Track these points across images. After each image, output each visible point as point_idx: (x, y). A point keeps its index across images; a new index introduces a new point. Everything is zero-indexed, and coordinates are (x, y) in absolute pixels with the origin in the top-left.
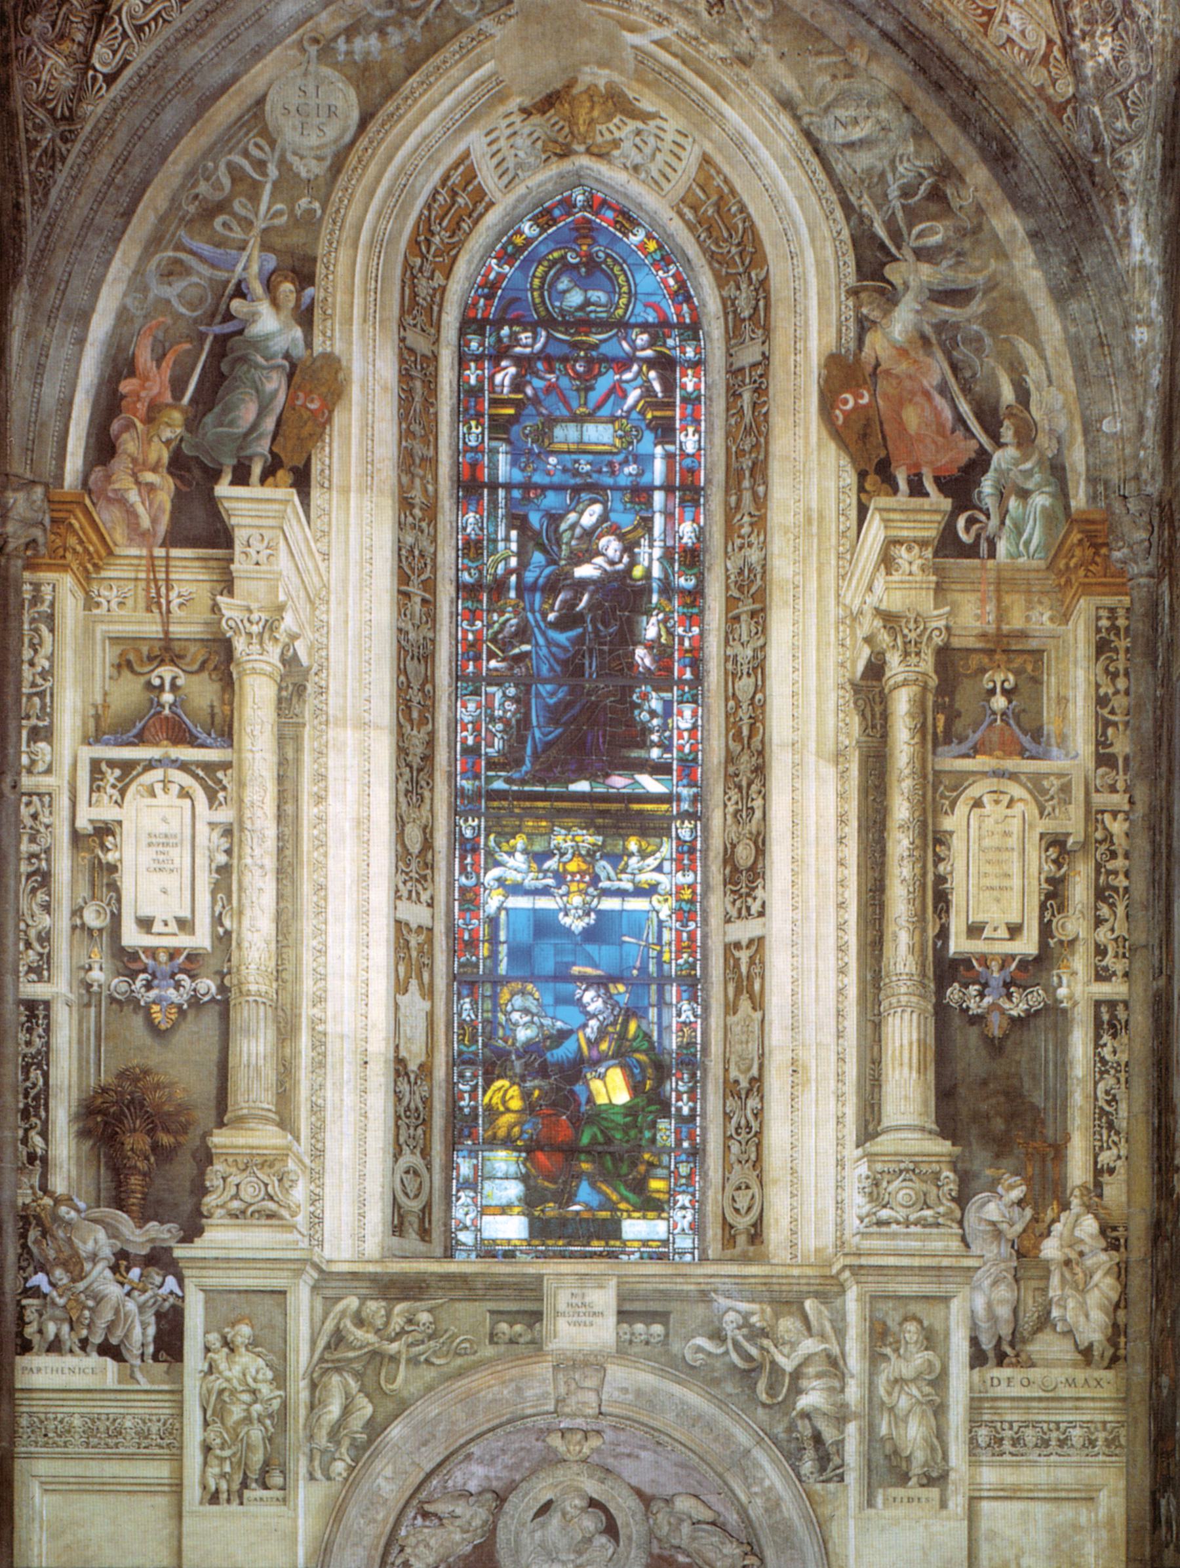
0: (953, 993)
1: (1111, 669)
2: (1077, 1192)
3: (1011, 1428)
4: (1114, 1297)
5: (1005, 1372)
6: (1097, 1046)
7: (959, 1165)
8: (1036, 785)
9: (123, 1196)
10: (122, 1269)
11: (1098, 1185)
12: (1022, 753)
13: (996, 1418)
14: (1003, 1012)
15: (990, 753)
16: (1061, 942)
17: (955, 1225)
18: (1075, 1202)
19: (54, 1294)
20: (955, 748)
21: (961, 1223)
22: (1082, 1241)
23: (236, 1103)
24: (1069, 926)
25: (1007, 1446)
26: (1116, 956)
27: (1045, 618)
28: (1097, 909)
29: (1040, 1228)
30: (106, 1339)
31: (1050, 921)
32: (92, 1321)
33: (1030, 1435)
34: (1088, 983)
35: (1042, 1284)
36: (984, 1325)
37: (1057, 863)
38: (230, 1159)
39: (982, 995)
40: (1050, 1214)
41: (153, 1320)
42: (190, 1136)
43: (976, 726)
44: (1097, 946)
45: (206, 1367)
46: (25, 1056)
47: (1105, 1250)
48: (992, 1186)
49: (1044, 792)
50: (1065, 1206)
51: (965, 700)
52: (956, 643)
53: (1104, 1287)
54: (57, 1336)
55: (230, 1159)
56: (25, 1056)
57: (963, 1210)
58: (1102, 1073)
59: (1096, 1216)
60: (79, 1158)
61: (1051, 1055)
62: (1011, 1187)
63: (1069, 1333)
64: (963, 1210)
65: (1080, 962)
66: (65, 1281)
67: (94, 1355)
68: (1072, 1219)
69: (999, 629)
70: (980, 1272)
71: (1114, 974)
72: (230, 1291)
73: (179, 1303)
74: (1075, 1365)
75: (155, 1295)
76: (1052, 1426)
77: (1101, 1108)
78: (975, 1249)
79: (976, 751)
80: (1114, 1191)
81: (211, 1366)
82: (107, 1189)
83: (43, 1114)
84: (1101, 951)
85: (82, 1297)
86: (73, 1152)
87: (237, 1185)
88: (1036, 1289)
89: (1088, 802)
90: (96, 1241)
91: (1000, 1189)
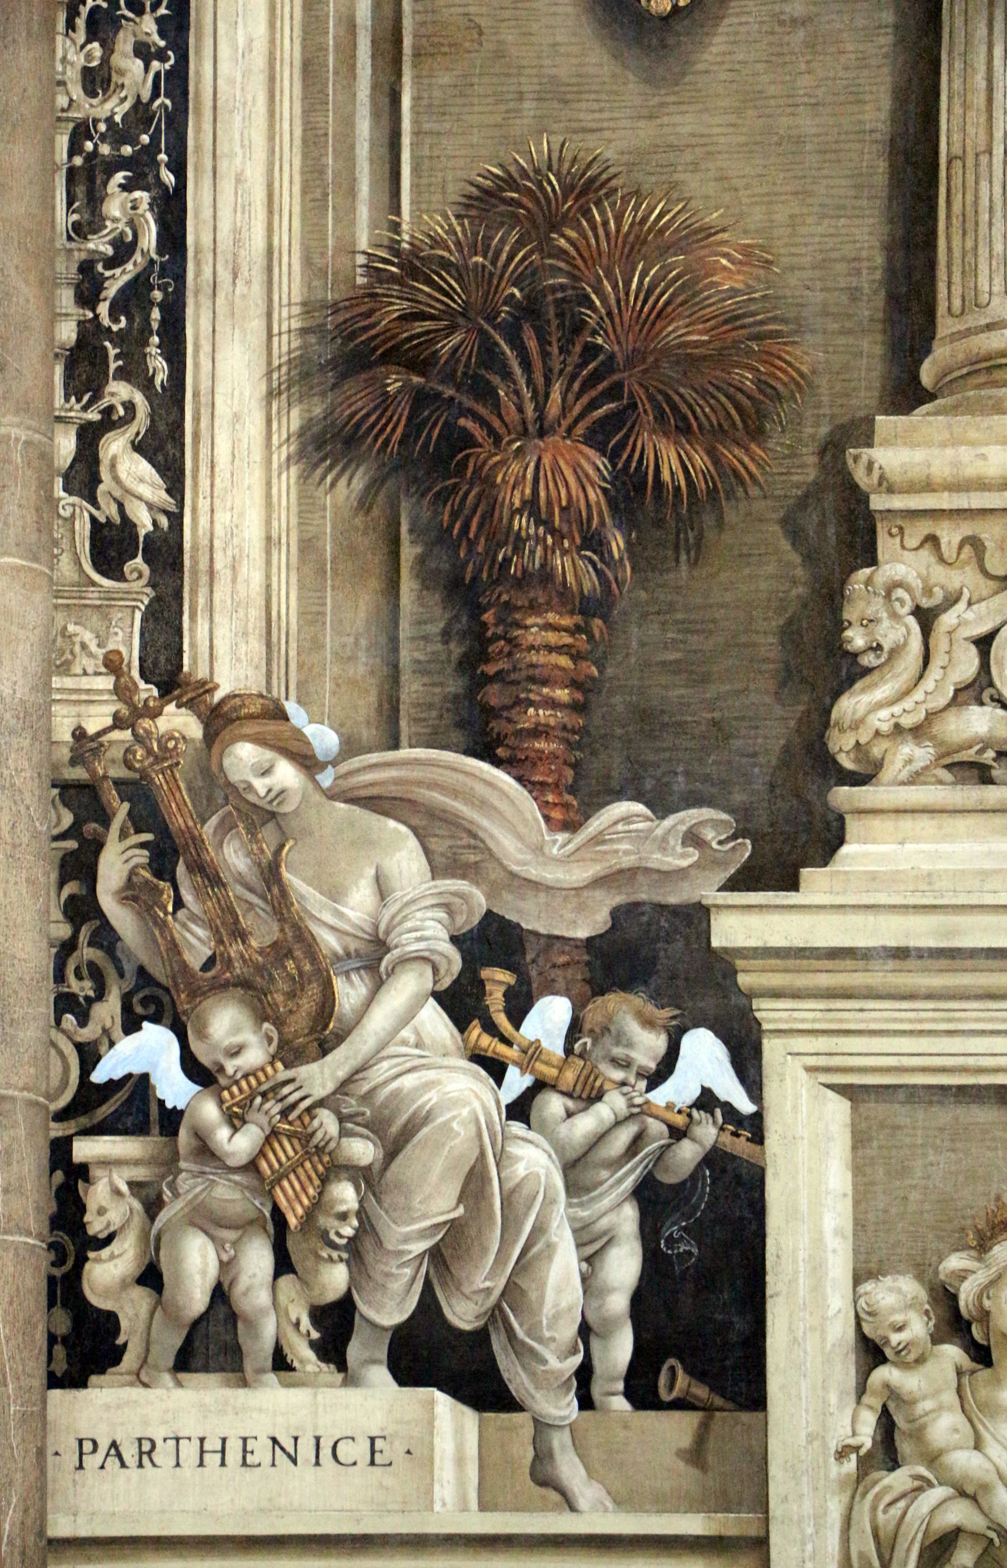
9: (494, 695)
10: (495, 1001)
19: (210, 1111)
23: (973, 303)
30: (429, 1305)
32: (367, 1226)
38: (950, 536)
41: (628, 1218)
42: (777, 441)
45: (866, 1435)
46: (82, 131)
54: (220, 1294)
55: (950, 536)
56: (82, 131)
60: (307, 546)
66: (255, 1056)
67: (380, 1375)
72: (963, 1093)
73: (741, 1146)
75: (639, 1112)
81: (887, 1425)
82: (421, 669)
83: (159, 366)
85: (327, 1123)
86: (286, 517)
87: (984, 643)
90: (382, 889)
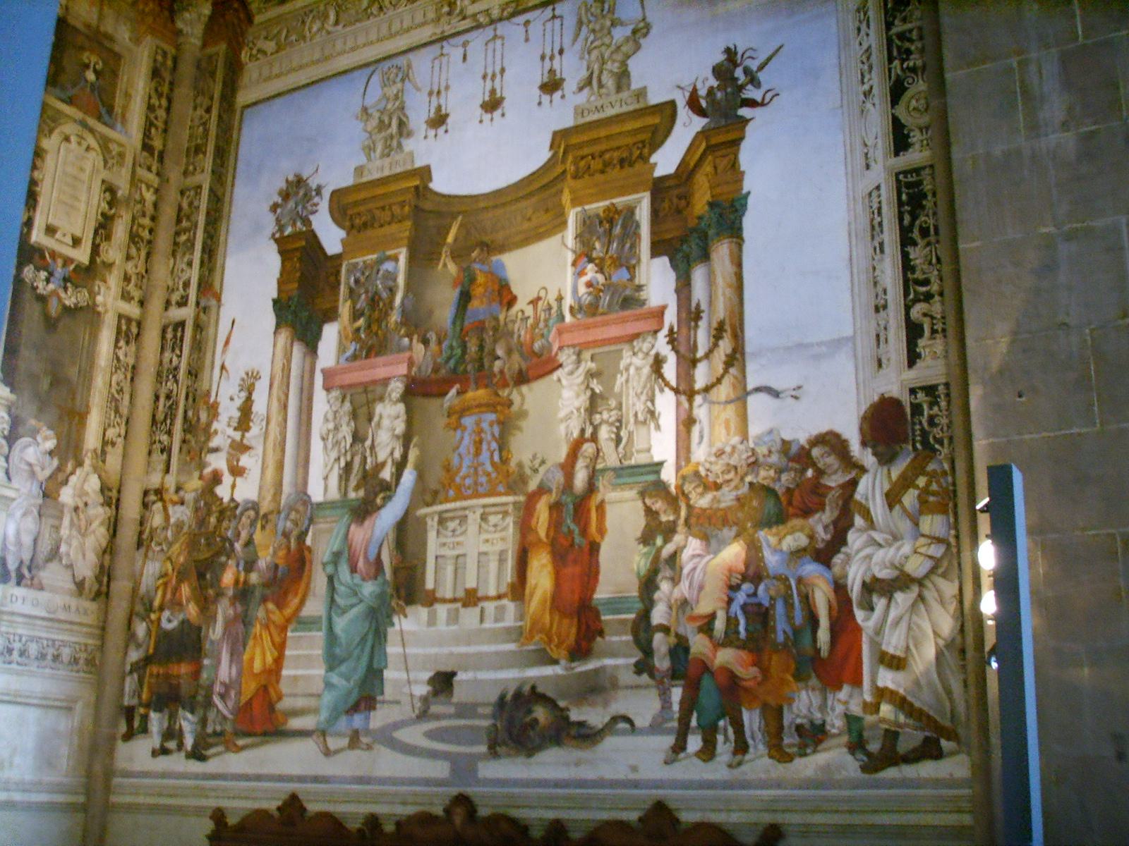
0: (28, 272)
1: (159, 89)
2: (89, 454)
3: (20, 641)
4: (104, 544)
5: (20, 592)
6: (116, 346)
7: (13, 410)
8: (105, 143)
11: (104, 452)
12: (99, 118)
13: (11, 630)
14: (59, 299)
15: (80, 109)
16: (103, 262)
17: (3, 459)
18: (87, 462)
20: (57, 91)
21: (7, 459)
22: (87, 494)
24: (111, 252)
25: (15, 654)
26: (136, 286)
27: (127, 36)
28: (129, 247)
29: (61, 477)
31: (99, 245)
33: (33, 649)
34: (115, 299)
35: (56, 523)
36: (12, 548)
37: (111, 204)
39: (48, 281)
40: (70, 467)
43: (74, 85)
44: (126, 274)
47: (103, 505)
48: (34, 433)
49: (109, 151)
50: (80, 464)
51: (68, 63)
52: (71, 21)
53: (99, 534)
57: (10, 447)
58: (117, 368)
59: (100, 477)
61: (86, 342)
62: (46, 438)
63: (70, 567)
64: (10, 447)
65: (114, 280)
68: (84, 474)
69: (98, 27)
70: (15, 503)
71: (133, 298)
74: (72, 595)
76: (50, 643)
77: (113, 396)
78: (16, 483)
79: (70, 101)
80: (114, 460)
84: (127, 279)
88: (53, 526)
89: (134, 172)
91: (39, 438)
